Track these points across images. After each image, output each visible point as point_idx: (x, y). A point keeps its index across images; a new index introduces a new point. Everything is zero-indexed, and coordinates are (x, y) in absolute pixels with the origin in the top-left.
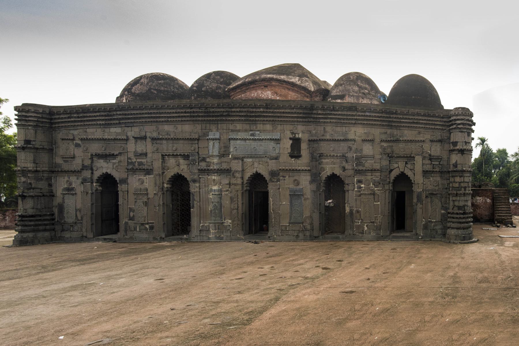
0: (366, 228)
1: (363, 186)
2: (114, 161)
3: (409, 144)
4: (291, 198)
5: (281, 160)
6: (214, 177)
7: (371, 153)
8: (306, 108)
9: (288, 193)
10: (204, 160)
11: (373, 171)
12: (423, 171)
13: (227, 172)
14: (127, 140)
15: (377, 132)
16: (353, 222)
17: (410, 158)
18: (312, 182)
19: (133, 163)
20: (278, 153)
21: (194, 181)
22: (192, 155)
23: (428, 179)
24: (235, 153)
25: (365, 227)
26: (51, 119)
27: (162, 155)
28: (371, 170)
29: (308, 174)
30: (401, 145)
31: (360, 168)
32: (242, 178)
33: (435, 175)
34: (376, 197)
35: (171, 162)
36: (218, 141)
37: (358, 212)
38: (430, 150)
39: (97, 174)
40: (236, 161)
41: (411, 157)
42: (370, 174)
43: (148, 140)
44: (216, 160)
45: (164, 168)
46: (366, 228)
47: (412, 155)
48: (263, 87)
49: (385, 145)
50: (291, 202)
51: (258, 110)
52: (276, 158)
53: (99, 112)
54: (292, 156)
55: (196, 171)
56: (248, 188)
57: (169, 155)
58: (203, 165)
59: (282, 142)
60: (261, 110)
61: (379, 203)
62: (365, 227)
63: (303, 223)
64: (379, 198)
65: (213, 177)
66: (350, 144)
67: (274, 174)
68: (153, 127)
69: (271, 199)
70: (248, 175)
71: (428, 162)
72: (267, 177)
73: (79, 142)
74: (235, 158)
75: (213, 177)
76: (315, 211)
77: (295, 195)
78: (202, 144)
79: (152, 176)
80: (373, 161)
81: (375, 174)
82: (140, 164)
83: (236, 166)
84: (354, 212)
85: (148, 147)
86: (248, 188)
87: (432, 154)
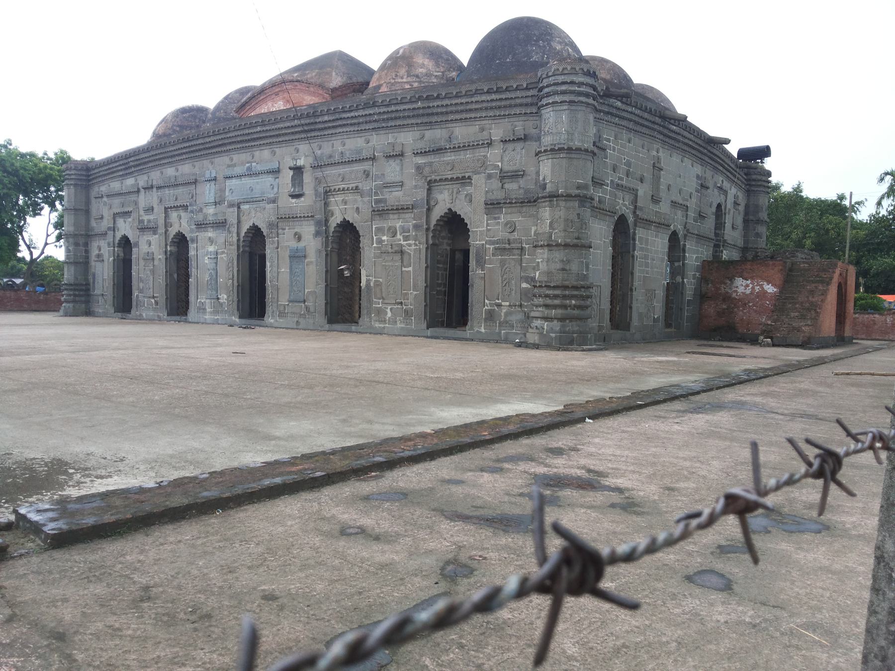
0: (389, 314)
1: (385, 238)
2: (130, 220)
3: (462, 152)
4: (291, 262)
5: (280, 204)
6: (210, 234)
7: (398, 179)
8: (308, 116)
9: (288, 253)
10: (201, 210)
11: (401, 209)
12: (486, 204)
13: (221, 225)
14: (138, 191)
15: (407, 139)
16: (370, 302)
17: (464, 180)
18: (317, 234)
19: (143, 221)
20: (277, 193)
21: (193, 241)
22: (191, 205)
23: (495, 218)
24: (230, 199)
25: (388, 311)
26: (89, 176)
27: (166, 208)
28: (397, 209)
29: (312, 222)
30: (449, 157)
31: (381, 206)
32: (238, 234)
33: (509, 210)
34: (406, 257)
35: (174, 215)
36: (213, 183)
37: (378, 284)
38: (502, 161)
39: (119, 236)
40: (231, 210)
41: (463, 178)
42: (396, 216)
43: (155, 189)
44: (211, 210)
45: (167, 225)
46: (389, 314)
47: (467, 175)
48: (273, 96)
49: (420, 160)
50: (291, 268)
51: (255, 130)
52: (274, 201)
53: (116, 162)
54: (293, 196)
55: (194, 227)
56: (247, 249)
57: (171, 207)
58: (200, 217)
59: (281, 175)
60: (259, 129)
61: (410, 269)
62: (388, 311)
63: (304, 301)
64: (410, 259)
65: (210, 234)
66: (366, 166)
67: (271, 225)
68: (158, 173)
69: (268, 264)
70: (245, 228)
71: (496, 184)
72: (265, 231)
73: (105, 199)
74: (231, 205)
75: (210, 234)
76: (320, 282)
77: (298, 257)
78: (200, 188)
79: (157, 236)
80: (400, 194)
81: (403, 216)
82: (149, 221)
83: (231, 216)
84: (372, 284)
85: (152, 199)
86: (247, 249)
87: (506, 168)
